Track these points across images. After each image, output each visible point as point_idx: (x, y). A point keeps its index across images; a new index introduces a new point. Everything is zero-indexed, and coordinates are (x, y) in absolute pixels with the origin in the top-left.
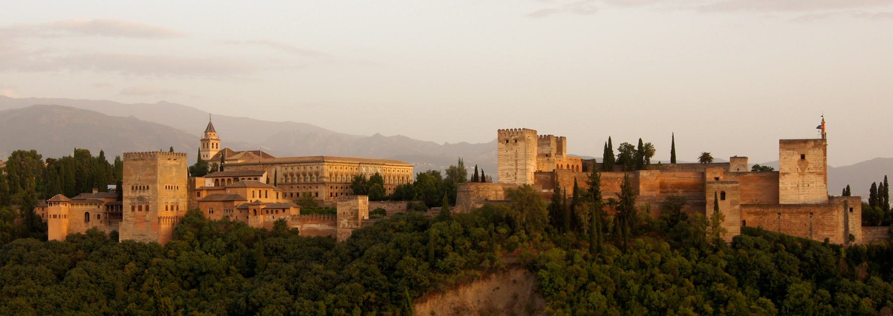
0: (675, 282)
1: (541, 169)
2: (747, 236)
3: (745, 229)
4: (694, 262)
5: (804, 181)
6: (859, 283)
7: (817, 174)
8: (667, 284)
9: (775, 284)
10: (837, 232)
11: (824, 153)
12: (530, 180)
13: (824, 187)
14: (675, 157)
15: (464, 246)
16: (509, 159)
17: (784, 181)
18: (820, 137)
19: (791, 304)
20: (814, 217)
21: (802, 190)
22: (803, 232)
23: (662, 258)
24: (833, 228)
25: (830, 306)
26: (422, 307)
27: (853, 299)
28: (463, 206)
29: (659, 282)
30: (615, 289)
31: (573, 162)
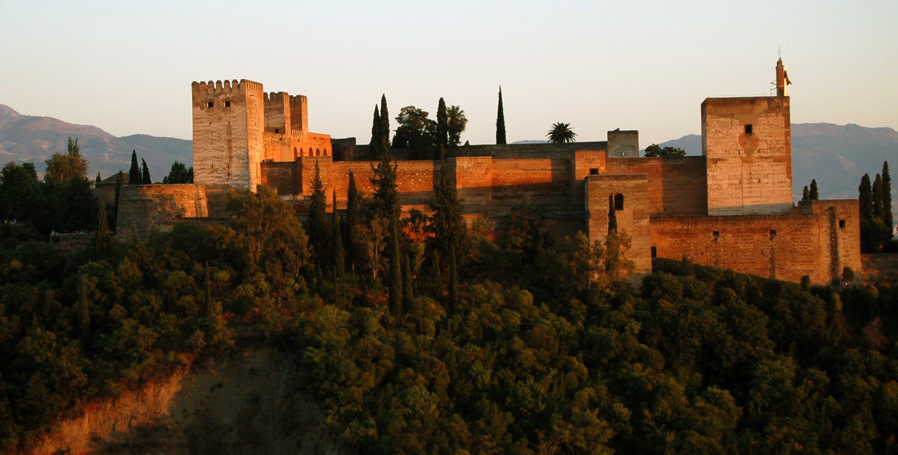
0: (552, 364)
1: (270, 157)
2: (670, 276)
3: (659, 265)
4: (580, 324)
5: (751, 174)
6: (877, 355)
7: (775, 161)
8: (539, 367)
9: (731, 362)
10: (819, 265)
11: (785, 122)
12: (256, 179)
13: (788, 184)
14: (505, 132)
15: (150, 307)
16: (216, 138)
17: (715, 174)
18: (774, 93)
19: (763, 397)
20: (777, 237)
21: (748, 190)
22: (759, 266)
23: (523, 320)
24: (812, 256)
25: (831, 399)
26: (75, 427)
27: (869, 384)
28: (133, 228)
29: (526, 364)
30: (449, 381)
31: (319, 142)
